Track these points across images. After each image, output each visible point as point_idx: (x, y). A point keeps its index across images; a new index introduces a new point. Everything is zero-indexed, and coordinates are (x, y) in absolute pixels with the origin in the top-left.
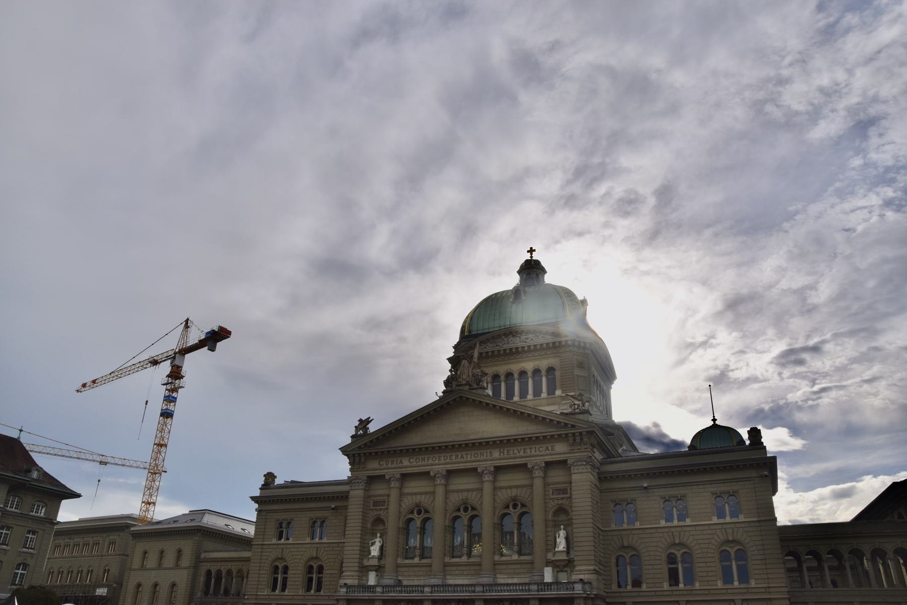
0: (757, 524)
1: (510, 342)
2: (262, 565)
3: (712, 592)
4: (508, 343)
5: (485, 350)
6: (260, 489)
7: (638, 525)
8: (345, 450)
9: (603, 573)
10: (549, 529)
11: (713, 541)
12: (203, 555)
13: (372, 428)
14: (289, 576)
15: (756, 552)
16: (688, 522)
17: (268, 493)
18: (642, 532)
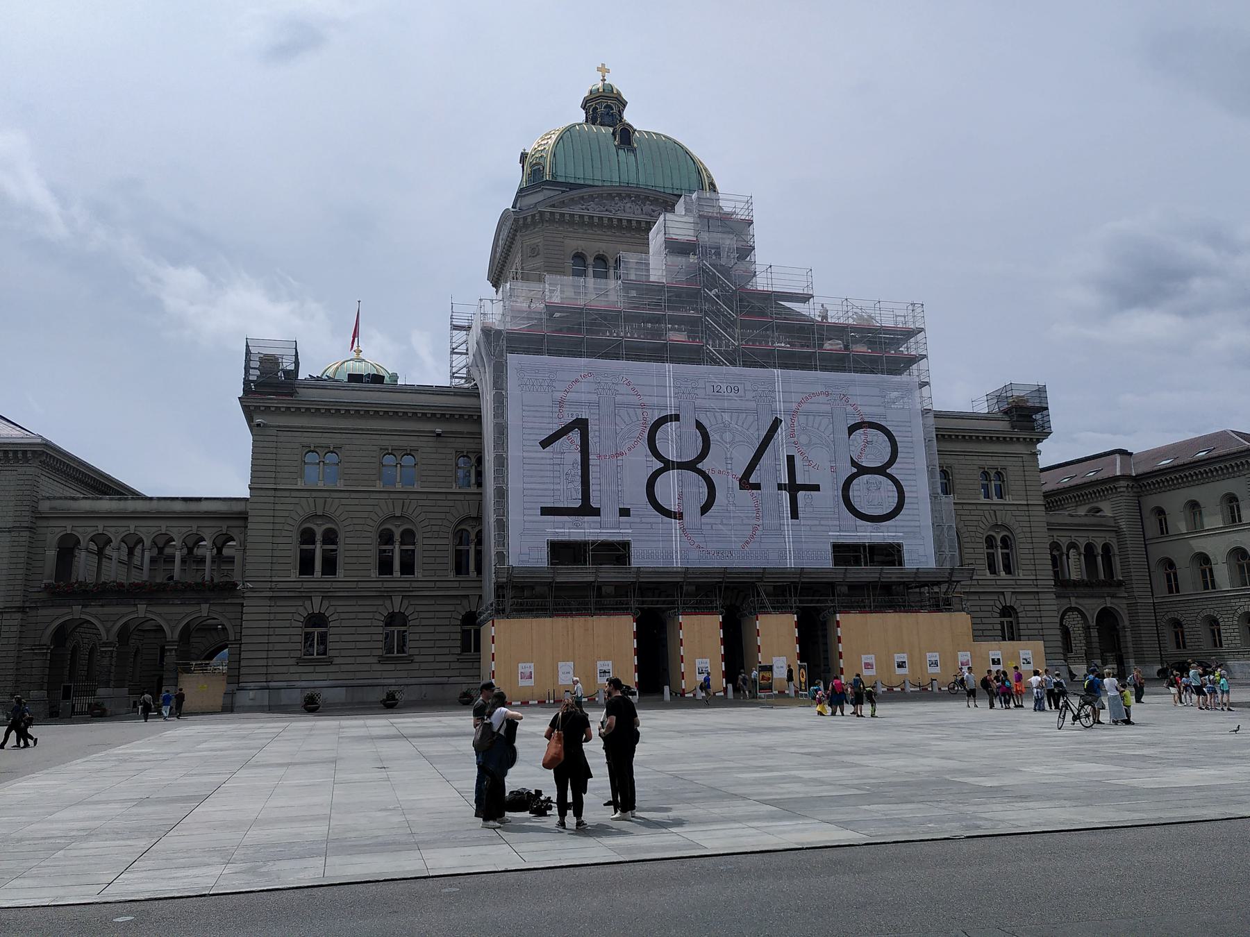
0: (1026, 508)
1: (628, 210)
2: (277, 527)
3: (980, 582)
5: (585, 213)
11: (981, 525)
12: (44, 506)
14: (341, 547)
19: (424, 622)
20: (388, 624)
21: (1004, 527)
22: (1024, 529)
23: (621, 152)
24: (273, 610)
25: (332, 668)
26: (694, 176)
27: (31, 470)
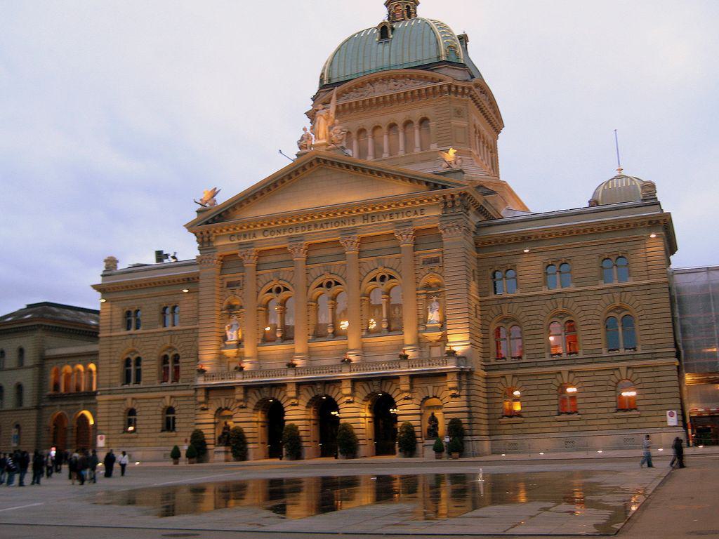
0: (647, 287)
2: (112, 358)
3: (596, 360)
4: (374, 91)
5: (349, 101)
6: (102, 276)
7: (518, 293)
8: (190, 227)
9: (481, 345)
10: (420, 302)
13: (221, 199)
14: (142, 368)
15: (644, 317)
16: (572, 288)
17: (111, 280)
18: (522, 300)
19: (183, 411)
20: (168, 413)
21: (619, 309)
22: (645, 307)
23: (380, 46)
24: (111, 406)
25: (138, 440)
26: (433, 47)
27: (39, 334)
